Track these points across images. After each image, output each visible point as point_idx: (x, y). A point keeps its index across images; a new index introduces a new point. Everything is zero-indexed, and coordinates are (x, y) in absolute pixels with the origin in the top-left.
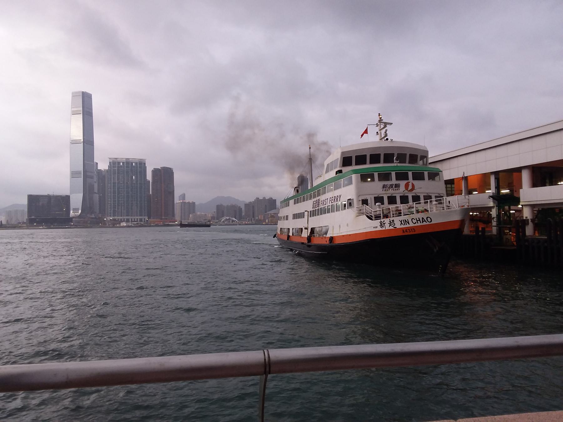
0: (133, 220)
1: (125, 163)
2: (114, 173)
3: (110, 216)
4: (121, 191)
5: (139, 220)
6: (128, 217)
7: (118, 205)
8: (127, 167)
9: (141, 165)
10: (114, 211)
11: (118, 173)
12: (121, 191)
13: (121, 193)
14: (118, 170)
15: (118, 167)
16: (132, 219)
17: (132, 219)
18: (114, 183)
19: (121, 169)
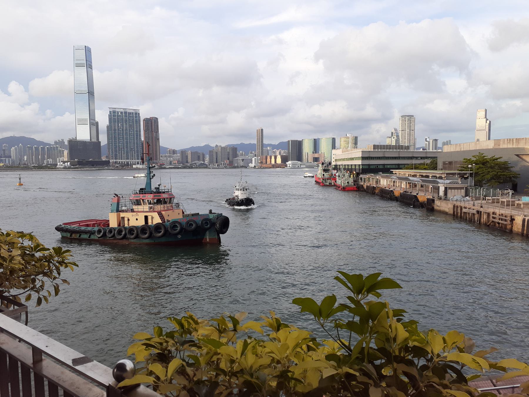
0: (132, 163)
1: (123, 113)
2: (115, 122)
3: (112, 159)
4: (121, 137)
5: (136, 163)
6: (127, 161)
7: (119, 150)
8: (126, 116)
9: (137, 114)
10: (116, 155)
11: (118, 122)
12: (121, 137)
13: (121, 140)
14: (118, 118)
15: (118, 116)
16: (131, 162)
17: (131, 162)
18: (115, 130)
19: (120, 118)
